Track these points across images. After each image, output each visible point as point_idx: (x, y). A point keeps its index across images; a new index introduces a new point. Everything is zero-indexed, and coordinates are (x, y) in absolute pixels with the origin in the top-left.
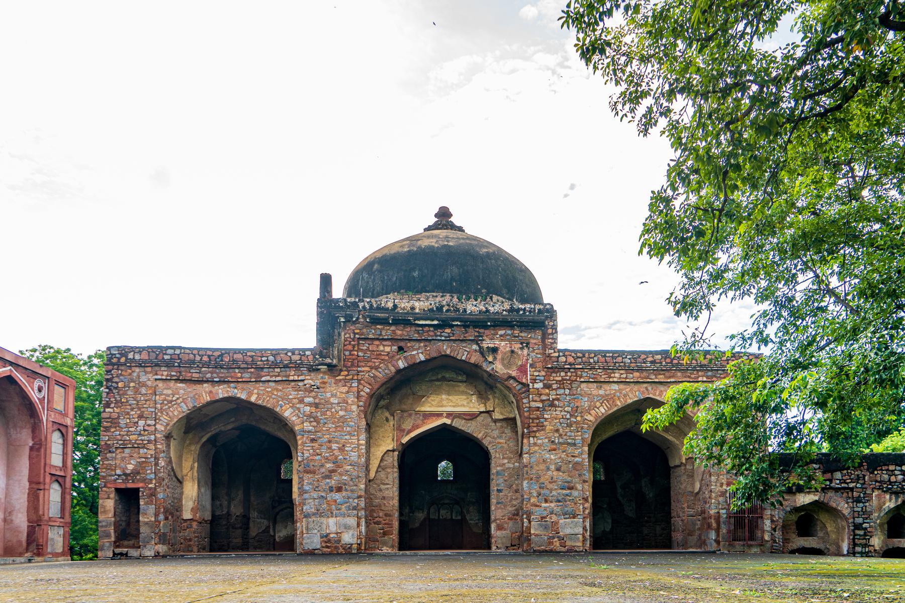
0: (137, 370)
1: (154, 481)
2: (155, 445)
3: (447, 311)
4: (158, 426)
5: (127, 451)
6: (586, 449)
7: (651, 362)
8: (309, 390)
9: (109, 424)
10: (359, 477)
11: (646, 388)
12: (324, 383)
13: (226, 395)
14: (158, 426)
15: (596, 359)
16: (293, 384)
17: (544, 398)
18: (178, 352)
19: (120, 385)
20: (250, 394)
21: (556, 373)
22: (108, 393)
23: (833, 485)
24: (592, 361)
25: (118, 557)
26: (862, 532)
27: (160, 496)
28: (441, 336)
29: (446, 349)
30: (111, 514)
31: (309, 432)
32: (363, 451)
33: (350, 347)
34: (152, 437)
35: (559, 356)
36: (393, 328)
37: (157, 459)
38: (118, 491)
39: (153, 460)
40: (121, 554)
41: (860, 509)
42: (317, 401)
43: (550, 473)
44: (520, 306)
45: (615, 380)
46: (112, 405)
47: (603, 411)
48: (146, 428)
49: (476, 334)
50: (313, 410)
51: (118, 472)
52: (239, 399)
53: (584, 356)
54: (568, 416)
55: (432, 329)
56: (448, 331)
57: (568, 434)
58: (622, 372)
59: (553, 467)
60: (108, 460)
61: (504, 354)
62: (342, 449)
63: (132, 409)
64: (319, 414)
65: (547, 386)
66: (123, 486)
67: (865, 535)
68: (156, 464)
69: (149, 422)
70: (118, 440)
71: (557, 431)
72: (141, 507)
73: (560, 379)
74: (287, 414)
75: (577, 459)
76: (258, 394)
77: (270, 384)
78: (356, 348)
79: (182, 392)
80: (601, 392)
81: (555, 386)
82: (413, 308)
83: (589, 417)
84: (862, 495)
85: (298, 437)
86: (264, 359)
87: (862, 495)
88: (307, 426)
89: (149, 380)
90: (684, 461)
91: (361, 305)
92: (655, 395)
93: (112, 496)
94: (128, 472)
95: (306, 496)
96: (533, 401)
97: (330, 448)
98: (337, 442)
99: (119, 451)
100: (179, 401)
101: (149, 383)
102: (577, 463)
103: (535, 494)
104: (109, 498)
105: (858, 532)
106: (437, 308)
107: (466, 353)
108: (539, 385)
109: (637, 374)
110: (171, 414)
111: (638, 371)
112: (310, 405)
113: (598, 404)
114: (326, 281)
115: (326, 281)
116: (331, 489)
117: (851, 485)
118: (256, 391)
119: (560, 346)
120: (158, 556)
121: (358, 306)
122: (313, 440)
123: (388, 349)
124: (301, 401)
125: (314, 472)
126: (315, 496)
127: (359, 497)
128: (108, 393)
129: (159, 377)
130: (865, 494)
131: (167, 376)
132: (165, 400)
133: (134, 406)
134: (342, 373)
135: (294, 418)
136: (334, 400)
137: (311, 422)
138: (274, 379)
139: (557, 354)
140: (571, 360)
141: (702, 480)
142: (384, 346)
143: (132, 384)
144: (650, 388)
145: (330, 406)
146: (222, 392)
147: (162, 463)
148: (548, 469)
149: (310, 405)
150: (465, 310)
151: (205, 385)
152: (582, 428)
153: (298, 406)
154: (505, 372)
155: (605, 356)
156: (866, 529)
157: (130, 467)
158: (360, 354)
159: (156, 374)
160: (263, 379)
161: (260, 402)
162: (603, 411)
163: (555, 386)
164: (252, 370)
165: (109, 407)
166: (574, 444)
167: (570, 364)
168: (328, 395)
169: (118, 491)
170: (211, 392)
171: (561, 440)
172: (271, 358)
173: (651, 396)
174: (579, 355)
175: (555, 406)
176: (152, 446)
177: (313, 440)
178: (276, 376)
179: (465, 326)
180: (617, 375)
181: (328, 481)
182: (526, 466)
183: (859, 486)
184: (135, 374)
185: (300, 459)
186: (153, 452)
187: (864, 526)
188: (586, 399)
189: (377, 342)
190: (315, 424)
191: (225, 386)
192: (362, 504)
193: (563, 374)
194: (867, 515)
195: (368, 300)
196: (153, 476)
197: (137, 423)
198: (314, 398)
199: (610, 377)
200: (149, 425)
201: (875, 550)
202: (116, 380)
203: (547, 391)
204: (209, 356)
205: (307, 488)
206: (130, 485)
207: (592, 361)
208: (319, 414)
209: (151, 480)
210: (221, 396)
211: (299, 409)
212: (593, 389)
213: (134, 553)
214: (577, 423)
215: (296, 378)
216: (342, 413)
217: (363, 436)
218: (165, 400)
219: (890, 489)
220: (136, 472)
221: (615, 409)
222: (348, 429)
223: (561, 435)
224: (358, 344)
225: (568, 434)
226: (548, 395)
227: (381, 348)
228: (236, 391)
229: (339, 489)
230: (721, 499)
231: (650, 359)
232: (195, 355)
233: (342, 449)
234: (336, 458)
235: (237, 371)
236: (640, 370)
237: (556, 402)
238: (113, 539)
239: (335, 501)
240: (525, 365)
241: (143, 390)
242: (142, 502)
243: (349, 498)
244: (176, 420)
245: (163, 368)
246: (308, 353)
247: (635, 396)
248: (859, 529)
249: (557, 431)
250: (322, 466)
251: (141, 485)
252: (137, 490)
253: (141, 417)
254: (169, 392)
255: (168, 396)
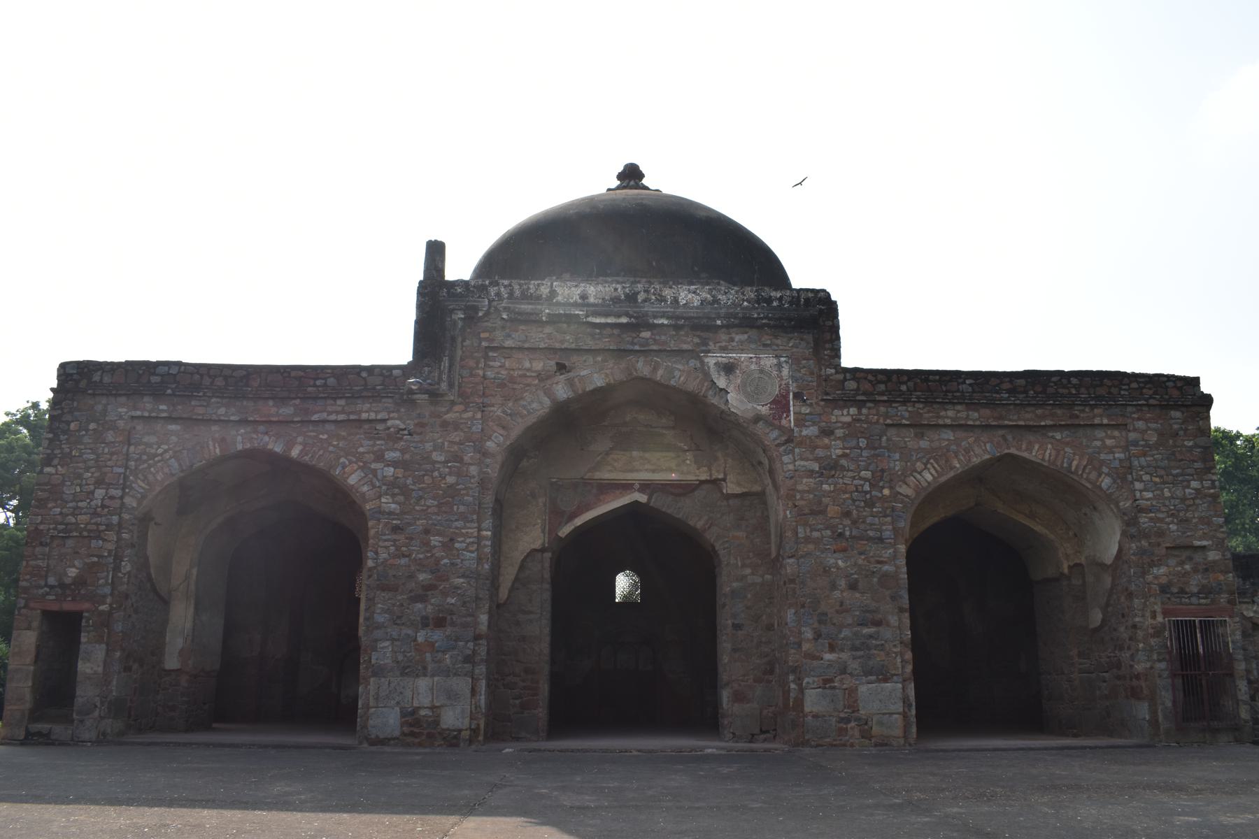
0: (104, 401)
1: (109, 600)
2: (119, 533)
3: (645, 301)
4: (127, 500)
5: (70, 543)
6: (902, 548)
7: (1008, 391)
8: (395, 437)
9: (45, 495)
10: (477, 598)
11: (1003, 436)
12: (422, 425)
13: (248, 446)
14: (127, 500)
15: (911, 384)
16: (366, 426)
17: (820, 453)
18: (174, 371)
19: (73, 426)
20: (290, 445)
21: (842, 408)
22: (51, 440)
24: (904, 388)
25: (31, 739)
27: (118, 627)
28: (633, 344)
29: (642, 367)
30: (29, 659)
31: (390, 513)
32: (488, 550)
33: (472, 363)
34: (115, 519)
35: (845, 380)
36: (548, 330)
37: (118, 558)
38: (47, 614)
39: (111, 560)
40: (40, 734)
42: (407, 456)
43: (837, 594)
44: (773, 294)
45: (948, 422)
46: (56, 462)
47: (929, 478)
48: (107, 502)
49: (696, 340)
50: (400, 473)
51: (52, 580)
52: (272, 454)
53: (889, 380)
54: (867, 488)
55: (616, 332)
56: (646, 334)
57: (869, 520)
58: (959, 407)
59: (842, 583)
60: (37, 559)
61: (747, 377)
62: (448, 545)
63: (87, 469)
64: (409, 481)
65: (827, 432)
66: (55, 607)
68: (117, 568)
69: (113, 492)
70: (57, 523)
71: (847, 514)
72: (82, 647)
73: (848, 419)
74: (352, 480)
75: (886, 568)
76: (305, 445)
77: (329, 427)
78: (482, 365)
79: (174, 439)
80: (924, 444)
81: (839, 433)
82: (584, 297)
83: (904, 490)
85: (370, 524)
86: (318, 383)
88: (388, 503)
89: (121, 417)
90: (1066, 571)
91: (493, 291)
92: (1019, 449)
93: (35, 624)
94: (68, 581)
95: (378, 634)
96: (802, 459)
97: (427, 544)
98: (439, 534)
99: (56, 542)
100: (167, 456)
101: (121, 423)
102: (885, 575)
103: (809, 635)
104: (29, 628)
106: (627, 296)
107: (678, 374)
108: (811, 431)
109: (987, 412)
110: (151, 477)
111: (986, 406)
112: (395, 464)
113: (919, 465)
114: (435, 252)
115: (435, 252)
116: (424, 623)
118: (300, 439)
119: (847, 361)
120: (102, 740)
121: (488, 293)
122: (396, 529)
123: (538, 366)
124: (379, 457)
125: (393, 589)
126: (395, 634)
127: (477, 638)
128: (51, 440)
129: (139, 413)
131: (150, 412)
132: (144, 453)
133: (91, 463)
134: (457, 408)
135: (365, 488)
136: (438, 457)
137: (393, 495)
138: (333, 417)
139: (840, 377)
140: (866, 386)
141: (1108, 605)
142: (531, 361)
143: (92, 426)
144: (1010, 437)
145: (428, 467)
146: (241, 440)
147: (126, 566)
148: (834, 586)
149: (395, 464)
150: (676, 300)
151: (215, 428)
152: (893, 509)
153: (373, 466)
154: (749, 406)
155: (927, 380)
157: (72, 572)
158: (489, 374)
159: (136, 409)
160: (315, 417)
161: (307, 458)
162: (929, 478)
163: (839, 433)
164: (298, 401)
165: (50, 465)
166: (881, 540)
167: (864, 394)
168: (429, 446)
169: (47, 614)
170: (223, 440)
171: (855, 532)
172: (331, 381)
173: (1013, 451)
174: (880, 377)
175: (843, 468)
176: (112, 536)
177: (396, 529)
178: (337, 413)
179: (677, 328)
180: (950, 413)
181: (419, 606)
182: (792, 581)
184: (99, 408)
185: (370, 563)
186: (111, 546)
188: (897, 456)
189: (521, 356)
190: (401, 498)
191: (249, 429)
192: (483, 651)
193: (853, 411)
195: (506, 282)
196: (107, 590)
197: (93, 493)
198: (403, 451)
199: (938, 417)
200: (112, 498)
202: (68, 417)
203: (826, 441)
204: (226, 378)
205: (380, 618)
206: (68, 606)
207: (904, 388)
208: (409, 481)
209: (104, 596)
210: (240, 447)
211: (374, 472)
212: (908, 439)
213: (58, 730)
214: (883, 499)
215: (373, 416)
216: (451, 480)
217: (488, 523)
218: (144, 453)
220: (80, 582)
221: (952, 474)
222: (462, 508)
223: (854, 522)
224: (486, 358)
225: (869, 520)
226: (828, 447)
227: (527, 365)
228: (266, 438)
229: (440, 623)
230: (1153, 641)
231: (1006, 386)
232: (202, 376)
233: (448, 545)
234: (438, 561)
235: (271, 403)
236: (991, 404)
237: (843, 462)
238: (28, 706)
239: (432, 645)
240: (786, 397)
241: (110, 436)
242: (83, 640)
243: (457, 639)
244: (158, 489)
245: (146, 399)
246: (395, 372)
247: (985, 451)
249: (847, 514)
250: (411, 576)
251: (86, 606)
252: (78, 616)
253: (99, 483)
254: (153, 439)
255: (149, 445)
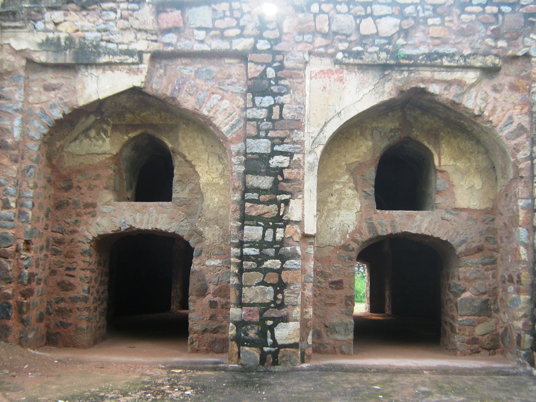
23: (184, 45)
26: (265, 182)
41: (262, 114)
67: (276, 189)
84: (271, 73)
87: (271, 73)
105: (254, 181)
117: (240, 45)
130: (281, 67)
156: (280, 171)
183: (263, 45)
187: (275, 161)
194: (281, 127)
201: (306, 236)
219: (358, 54)
248: (255, 173)
